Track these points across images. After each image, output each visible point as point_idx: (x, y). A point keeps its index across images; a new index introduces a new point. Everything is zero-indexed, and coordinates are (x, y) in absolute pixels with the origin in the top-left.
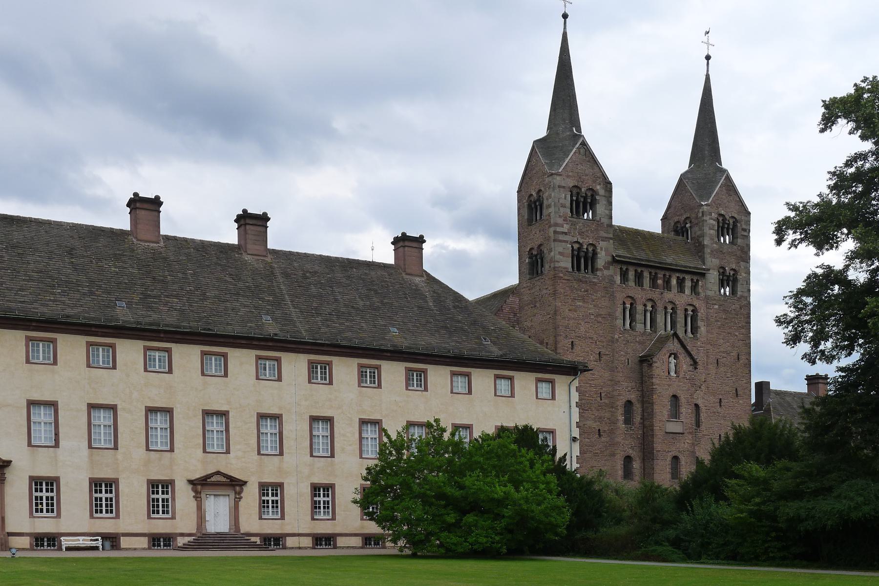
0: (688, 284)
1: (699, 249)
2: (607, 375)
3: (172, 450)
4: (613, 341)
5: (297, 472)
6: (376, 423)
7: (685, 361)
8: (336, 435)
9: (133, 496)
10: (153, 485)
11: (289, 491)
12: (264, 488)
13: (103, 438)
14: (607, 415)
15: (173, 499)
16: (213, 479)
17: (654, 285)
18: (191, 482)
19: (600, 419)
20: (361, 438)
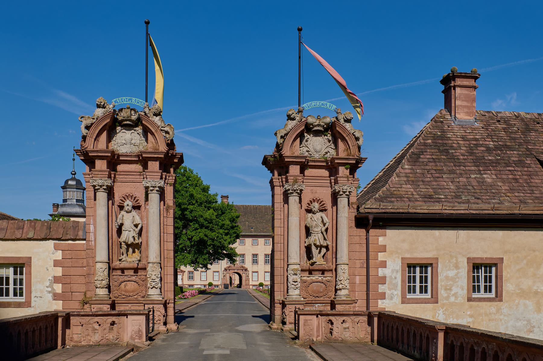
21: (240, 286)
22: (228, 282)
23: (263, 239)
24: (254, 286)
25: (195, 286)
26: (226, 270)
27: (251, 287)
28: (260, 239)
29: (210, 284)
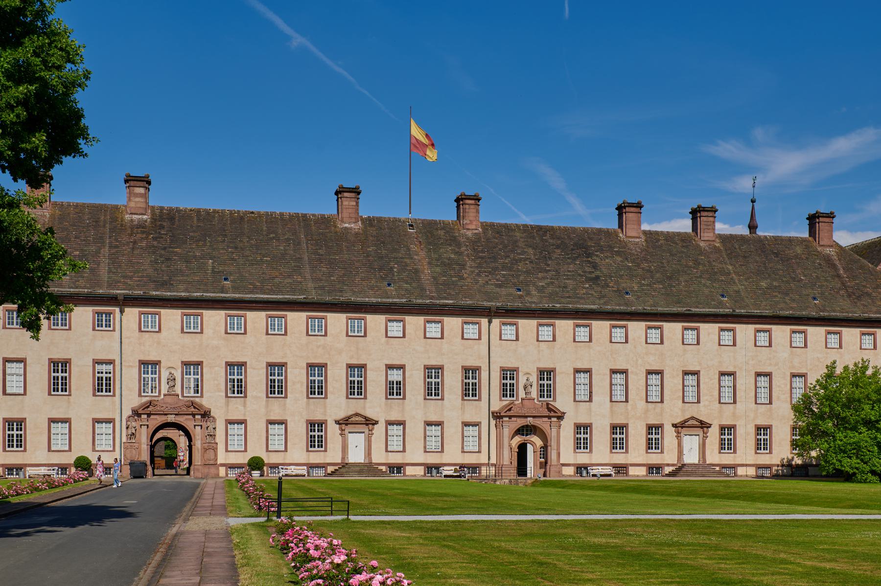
3: (662, 401)
5: (746, 417)
6: (803, 375)
8: (774, 386)
9: (637, 436)
10: (650, 428)
11: (740, 431)
12: (722, 428)
13: (619, 395)
15: (662, 438)
16: (689, 423)
18: (675, 426)
20: (791, 388)
22: (145, 457)
23: (263, 314)
24: (232, 467)
25: (30, 471)
26: (136, 413)
27: (222, 471)
28: (251, 315)
29: (83, 464)
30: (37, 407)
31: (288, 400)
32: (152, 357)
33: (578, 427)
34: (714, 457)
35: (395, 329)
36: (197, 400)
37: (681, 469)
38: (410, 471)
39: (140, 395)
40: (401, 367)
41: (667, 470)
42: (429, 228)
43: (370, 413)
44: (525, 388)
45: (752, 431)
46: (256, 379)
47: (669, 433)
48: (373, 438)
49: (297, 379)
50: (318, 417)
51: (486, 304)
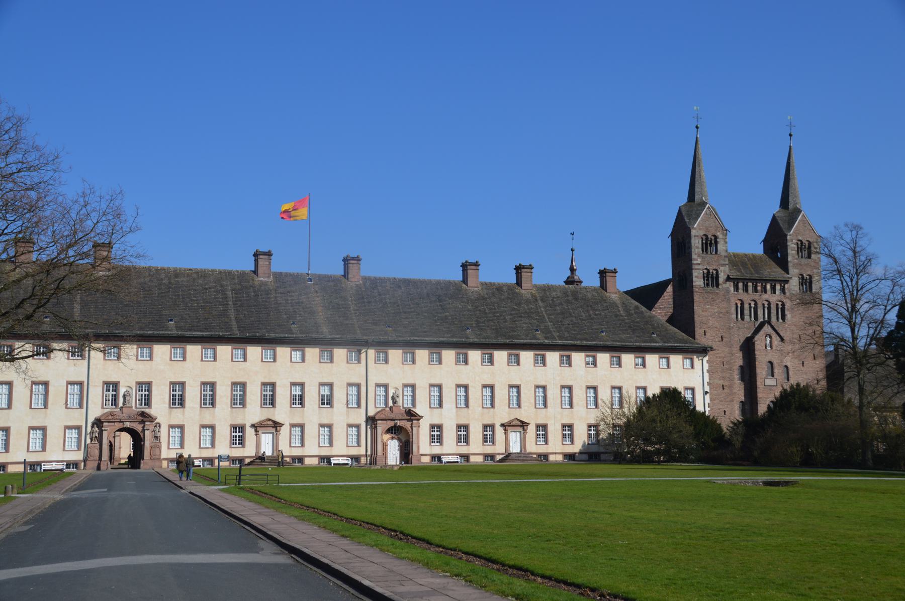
0: (778, 287)
1: (784, 265)
2: (727, 349)
4: (730, 328)
5: (555, 416)
7: (776, 340)
9: (476, 433)
12: (538, 426)
14: (728, 375)
17: (756, 291)
18: (503, 425)
19: (724, 378)
21: (135, 461)
27: (165, 464)
30: (20, 418)
31: (216, 410)
32: (113, 379)
33: (433, 426)
34: (533, 447)
35: (297, 355)
36: (147, 411)
37: (508, 457)
38: (307, 461)
39: (102, 407)
40: (302, 385)
41: (498, 458)
42: (323, 280)
43: (278, 419)
44: (393, 398)
45: (560, 428)
46: (193, 395)
47: (499, 431)
48: (280, 437)
49: (224, 394)
50: (239, 422)
51: (365, 338)
